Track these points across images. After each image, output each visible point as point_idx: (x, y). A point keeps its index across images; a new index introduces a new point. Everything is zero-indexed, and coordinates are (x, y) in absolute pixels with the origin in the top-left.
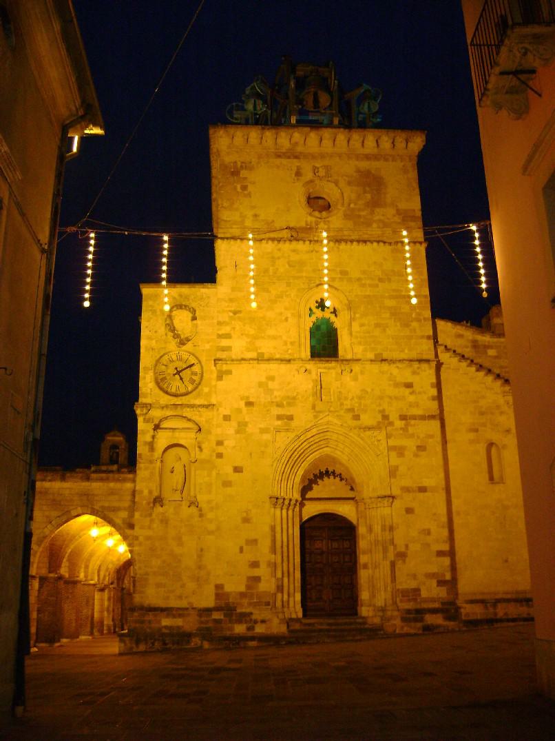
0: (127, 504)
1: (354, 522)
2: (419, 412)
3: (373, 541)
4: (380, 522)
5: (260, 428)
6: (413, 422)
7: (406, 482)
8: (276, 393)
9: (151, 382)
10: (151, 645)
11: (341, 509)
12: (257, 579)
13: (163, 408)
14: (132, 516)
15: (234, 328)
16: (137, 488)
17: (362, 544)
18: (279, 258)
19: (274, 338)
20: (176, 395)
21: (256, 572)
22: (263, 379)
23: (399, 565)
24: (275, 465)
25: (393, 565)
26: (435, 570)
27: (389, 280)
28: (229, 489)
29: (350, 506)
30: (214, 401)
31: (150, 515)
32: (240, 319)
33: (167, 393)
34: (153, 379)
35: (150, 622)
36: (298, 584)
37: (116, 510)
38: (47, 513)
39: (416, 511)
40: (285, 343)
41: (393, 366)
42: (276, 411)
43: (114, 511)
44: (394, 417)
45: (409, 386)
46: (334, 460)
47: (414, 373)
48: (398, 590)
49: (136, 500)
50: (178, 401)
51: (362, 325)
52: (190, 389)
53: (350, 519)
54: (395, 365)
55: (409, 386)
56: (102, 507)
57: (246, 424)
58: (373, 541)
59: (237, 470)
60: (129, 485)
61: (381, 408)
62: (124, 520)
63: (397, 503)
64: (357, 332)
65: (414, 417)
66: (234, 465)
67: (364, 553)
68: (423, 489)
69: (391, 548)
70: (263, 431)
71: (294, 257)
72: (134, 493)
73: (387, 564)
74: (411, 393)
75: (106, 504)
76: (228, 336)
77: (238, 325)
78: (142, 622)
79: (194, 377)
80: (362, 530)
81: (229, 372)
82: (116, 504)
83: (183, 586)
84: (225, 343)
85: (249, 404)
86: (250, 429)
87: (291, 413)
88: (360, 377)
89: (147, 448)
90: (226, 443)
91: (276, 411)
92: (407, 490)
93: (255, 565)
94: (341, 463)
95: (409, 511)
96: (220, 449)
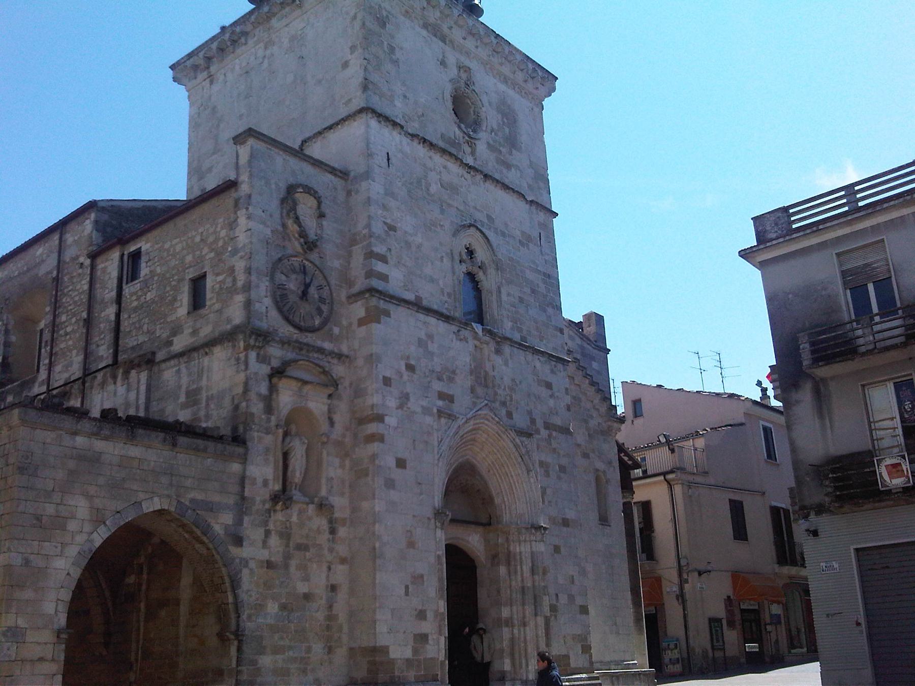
0: (231, 500)
9: (266, 297)
14: (239, 522)
16: (248, 473)
28: (392, 492)
30: (345, 349)
31: (266, 523)
37: (210, 507)
38: (98, 503)
42: (437, 386)
43: (211, 510)
49: (247, 494)
56: (192, 501)
60: (236, 467)
62: (226, 527)
72: (242, 480)
75: (199, 496)
82: (216, 498)
89: (261, 406)
91: (437, 386)
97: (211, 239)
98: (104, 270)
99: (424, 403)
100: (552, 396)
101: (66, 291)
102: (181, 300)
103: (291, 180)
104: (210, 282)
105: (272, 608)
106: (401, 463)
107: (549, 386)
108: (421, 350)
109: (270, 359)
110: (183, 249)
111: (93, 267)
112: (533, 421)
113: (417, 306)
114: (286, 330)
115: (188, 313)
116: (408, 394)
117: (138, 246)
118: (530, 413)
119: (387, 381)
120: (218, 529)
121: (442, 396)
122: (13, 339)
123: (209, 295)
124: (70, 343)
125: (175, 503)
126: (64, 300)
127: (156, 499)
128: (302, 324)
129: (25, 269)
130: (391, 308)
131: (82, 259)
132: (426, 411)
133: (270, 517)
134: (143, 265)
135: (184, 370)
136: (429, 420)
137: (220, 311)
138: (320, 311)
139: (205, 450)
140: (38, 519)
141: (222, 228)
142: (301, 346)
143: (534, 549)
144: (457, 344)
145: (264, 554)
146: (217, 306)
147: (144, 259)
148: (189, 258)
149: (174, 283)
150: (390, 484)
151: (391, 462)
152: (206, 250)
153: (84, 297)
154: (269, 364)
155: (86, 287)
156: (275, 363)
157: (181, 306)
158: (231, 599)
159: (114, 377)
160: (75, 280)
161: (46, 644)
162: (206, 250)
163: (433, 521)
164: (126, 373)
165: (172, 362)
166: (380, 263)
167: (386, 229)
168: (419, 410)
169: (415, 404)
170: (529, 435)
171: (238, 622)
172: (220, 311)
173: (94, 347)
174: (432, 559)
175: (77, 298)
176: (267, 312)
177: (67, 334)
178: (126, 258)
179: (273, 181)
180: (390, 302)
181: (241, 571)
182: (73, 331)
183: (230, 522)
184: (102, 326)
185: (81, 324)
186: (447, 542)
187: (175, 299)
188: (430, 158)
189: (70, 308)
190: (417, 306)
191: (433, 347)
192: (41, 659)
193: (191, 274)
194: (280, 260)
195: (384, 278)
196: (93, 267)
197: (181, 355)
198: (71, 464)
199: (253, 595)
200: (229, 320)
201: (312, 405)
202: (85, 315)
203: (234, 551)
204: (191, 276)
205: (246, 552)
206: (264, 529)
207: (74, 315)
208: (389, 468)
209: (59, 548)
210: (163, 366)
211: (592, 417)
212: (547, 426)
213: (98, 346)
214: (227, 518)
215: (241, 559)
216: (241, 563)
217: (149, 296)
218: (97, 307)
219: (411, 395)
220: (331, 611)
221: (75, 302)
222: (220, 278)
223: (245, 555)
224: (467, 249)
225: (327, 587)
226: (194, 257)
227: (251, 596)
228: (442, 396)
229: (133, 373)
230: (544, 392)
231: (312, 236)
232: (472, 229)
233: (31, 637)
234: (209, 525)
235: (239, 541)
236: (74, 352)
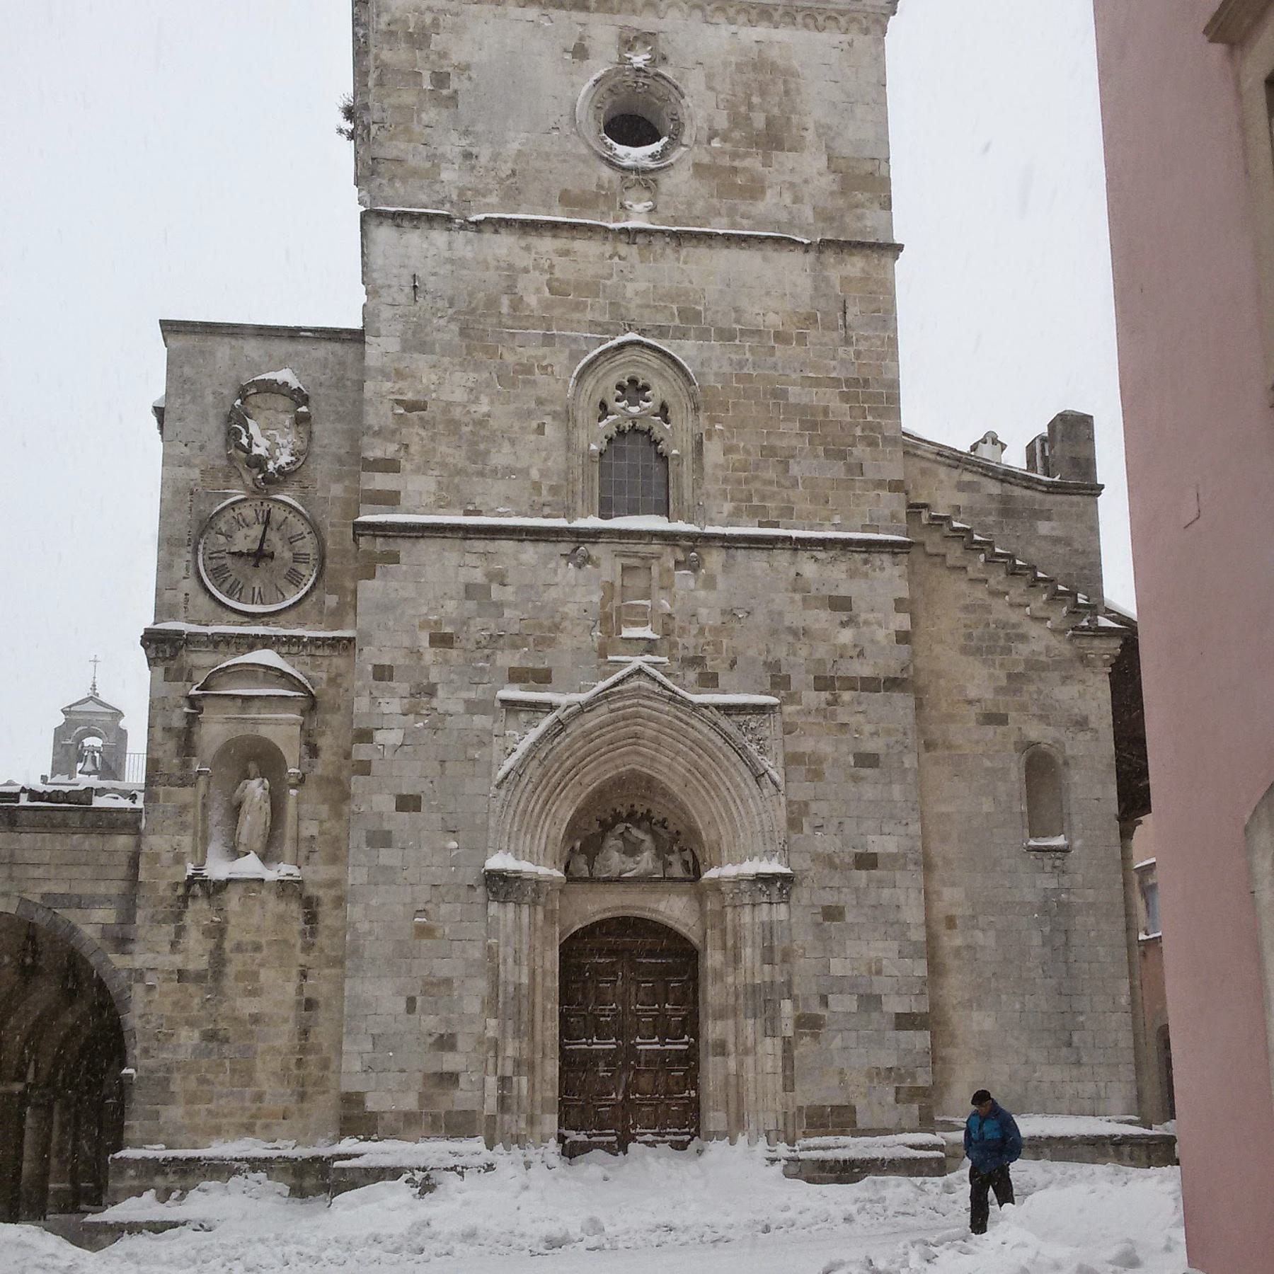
1: (695, 940)
2: (863, 669)
3: (741, 989)
4: (759, 940)
5: (468, 702)
6: (846, 696)
7: (826, 842)
8: (508, 613)
11: (662, 907)
12: (449, 1079)
13: (216, 644)
14: (128, 917)
15: (407, 446)
16: (145, 848)
17: (713, 994)
18: (526, 270)
19: (509, 471)
21: (451, 1062)
22: (478, 576)
23: (805, 1047)
24: (503, 793)
25: (788, 1045)
26: (892, 1062)
27: (802, 339)
29: (685, 899)
31: (179, 916)
32: (424, 423)
34: (192, 571)
36: (552, 1093)
37: (79, 903)
39: (850, 917)
40: (537, 487)
41: (803, 556)
44: (801, 679)
45: (840, 604)
46: (648, 785)
47: (852, 574)
48: (800, 1109)
49: (142, 876)
51: (728, 450)
53: (683, 930)
54: (807, 554)
55: (840, 604)
56: (44, 896)
57: (431, 691)
58: (741, 989)
59: (408, 803)
61: (770, 659)
62: (105, 928)
63: (802, 894)
64: (716, 466)
65: (851, 683)
66: (397, 792)
67: (721, 1015)
68: (867, 861)
69: (787, 1006)
70: (473, 707)
71: (565, 271)
73: (770, 1048)
74: (843, 625)
76: (390, 466)
77: (415, 435)
79: (302, 569)
80: (713, 959)
81: (394, 558)
82: (86, 889)
83: (259, 1097)
84: (380, 482)
85: (442, 640)
86: (446, 701)
87: (546, 665)
88: (721, 582)
90: (379, 736)
92: (829, 861)
93: (446, 1043)
94: (665, 793)
95: (832, 913)
96: (362, 752)
105: (189, 1038)
119: (382, 673)
120: (89, 931)
125: (16, 902)
133: (186, 907)
145: (178, 960)
150: (381, 839)
151: (385, 803)
168: (460, 708)
176: (187, 601)
180: (422, 537)
199: (153, 1019)
201: (265, 731)
203: (118, 961)
205: (140, 959)
214: (105, 915)
220: (307, 1039)
223: (137, 965)
225: (299, 1003)
227: (148, 1022)
235: (122, 943)
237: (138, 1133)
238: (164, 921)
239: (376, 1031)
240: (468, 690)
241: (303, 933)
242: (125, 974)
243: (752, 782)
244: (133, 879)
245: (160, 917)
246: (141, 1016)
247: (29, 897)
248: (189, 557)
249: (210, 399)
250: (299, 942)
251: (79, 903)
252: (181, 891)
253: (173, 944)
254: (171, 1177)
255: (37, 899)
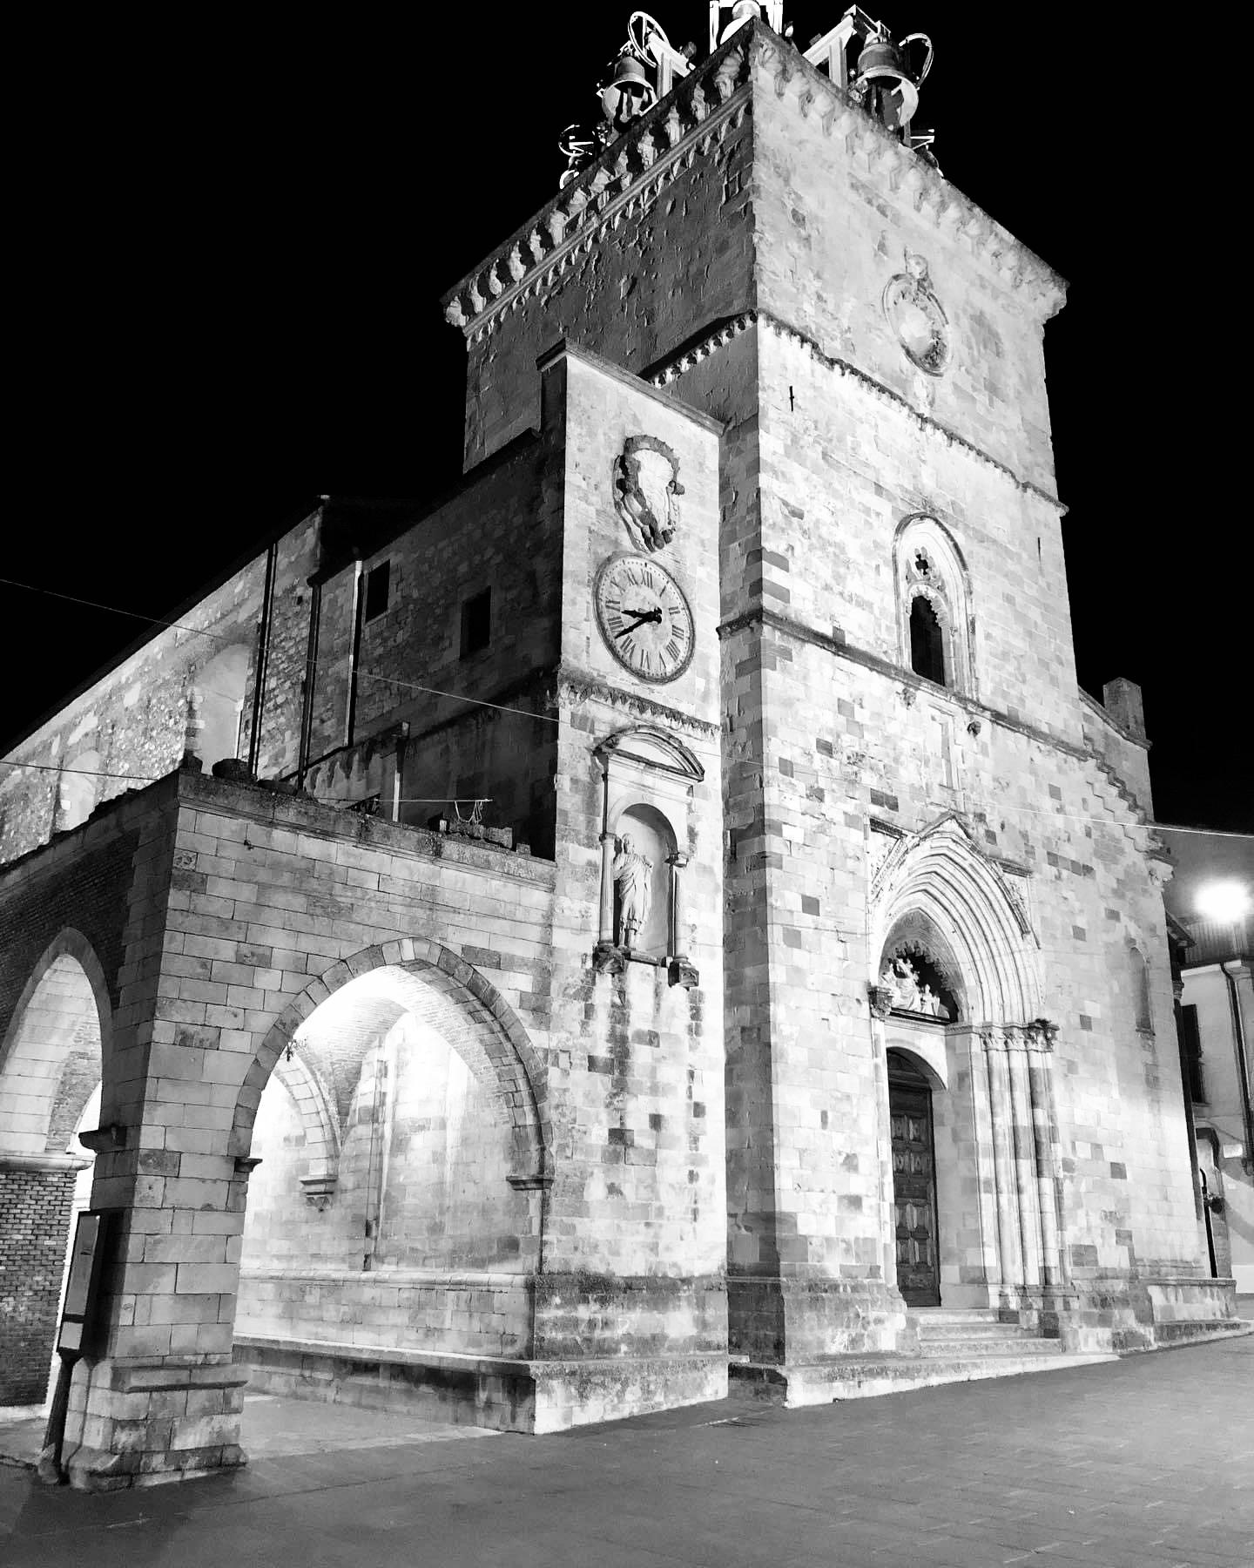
0: (530, 951)
10: (616, 1400)
20: (641, 676)
33: (624, 665)
34: (592, 615)
35: (592, 1324)
37: (497, 963)
43: (498, 966)
50: (642, 690)
52: (670, 667)
60: (537, 897)
62: (523, 997)
75: (478, 941)
78: (576, 1323)
82: (503, 947)
91: (869, 780)
97: (499, 532)
98: (334, 601)
99: (850, 807)
100: (1060, 810)
101: (277, 641)
102: (450, 638)
103: (632, 431)
104: (496, 602)
106: (811, 906)
107: (1055, 793)
108: (842, 719)
109: (593, 723)
110: (455, 554)
111: (316, 600)
112: (1030, 852)
113: (836, 644)
114: (622, 680)
115: (462, 658)
116: (822, 791)
117: (384, 560)
118: (1025, 836)
121: (877, 799)
122: (200, 724)
123: (494, 623)
124: (282, 720)
125: (437, 951)
126: (273, 656)
127: (407, 943)
128: (645, 669)
129: (219, 615)
130: (794, 646)
131: (299, 591)
132: (851, 821)
133: (594, 983)
134: (392, 587)
135: (454, 748)
136: (856, 836)
137: (510, 648)
138: (672, 650)
139: (487, 866)
140: (204, 966)
141: (515, 514)
142: (642, 704)
143: (1034, 1065)
144: (901, 709)
146: (507, 641)
147: (393, 580)
148: (463, 568)
149: (438, 611)
152: (490, 552)
153: (303, 647)
154: (592, 732)
155: (306, 633)
156: (603, 732)
157: (451, 644)
158: (530, 1120)
159: (347, 767)
160: (290, 624)
161: (215, 1181)
162: (490, 552)
163: (866, 1005)
164: (366, 760)
165: (436, 737)
166: (775, 569)
167: (786, 512)
168: (840, 818)
169: (834, 808)
170: (1024, 872)
171: (542, 1157)
172: (510, 648)
173: (316, 723)
174: (866, 1070)
175: (292, 651)
177: (277, 707)
178: (366, 579)
179: (600, 431)
181: (546, 1072)
182: (287, 702)
183: (529, 989)
184: (329, 689)
185: (299, 689)
186: (890, 1045)
187: (441, 638)
188: (861, 401)
189: (281, 667)
190: (836, 644)
191: (861, 715)
192: (208, 1208)
193: (466, 594)
194: (609, 560)
195: (783, 595)
196: (316, 600)
197: (450, 723)
198: (263, 876)
199: (568, 1112)
200: (526, 660)
202: (303, 674)
204: (465, 597)
206: (583, 1004)
207: (288, 677)
208: (791, 912)
209: (241, 1016)
210: (422, 744)
211: (1122, 851)
212: (1053, 859)
213: (323, 721)
215: (546, 1052)
216: (546, 1058)
217: (401, 636)
218: (321, 663)
219: (826, 793)
220: (697, 1149)
221: (290, 658)
222: (510, 595)
223: (553, 1045)
224: (919, 556)
226: (470, 566)
227: (564, 1115)
228: (877, 799)
229: (376, 758)
230: (1048, 803)
231: (662, 525)
232: (929, 523)
233: (188, 1167)
234: (493, 992)
236: (288, 734)
237: (556, 1251)
238: (575, 997)
239: (801, 1146)
240: (845, 802)
241: (690, 1029)
242: (541, 1054)
243: (1018, 933)
244: (548, 947)
245: (571, 991)
246: (557, 1107)
247: (450, 946)
248: (590, 598)
249: (601, 438)
250: (685, 1037)
251: (498, 962)
252: (589, 964)
253: (584, 1024)
254: (595, 1307)
255: (458, 952)
